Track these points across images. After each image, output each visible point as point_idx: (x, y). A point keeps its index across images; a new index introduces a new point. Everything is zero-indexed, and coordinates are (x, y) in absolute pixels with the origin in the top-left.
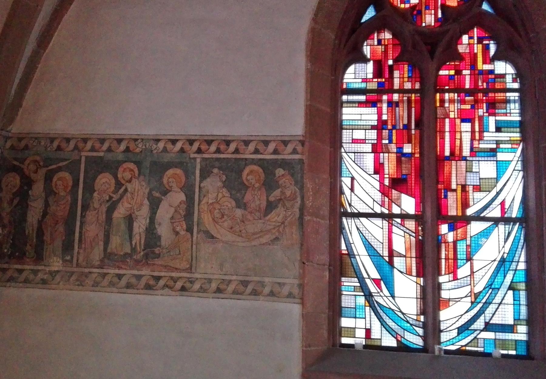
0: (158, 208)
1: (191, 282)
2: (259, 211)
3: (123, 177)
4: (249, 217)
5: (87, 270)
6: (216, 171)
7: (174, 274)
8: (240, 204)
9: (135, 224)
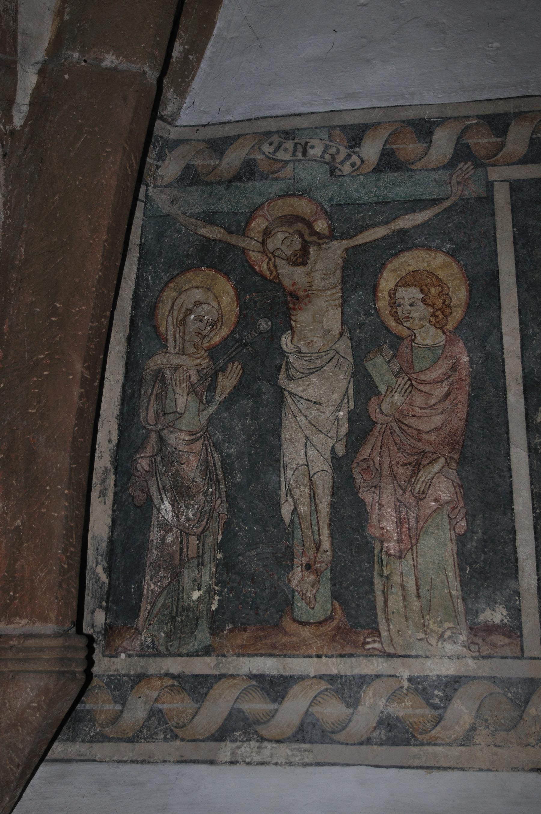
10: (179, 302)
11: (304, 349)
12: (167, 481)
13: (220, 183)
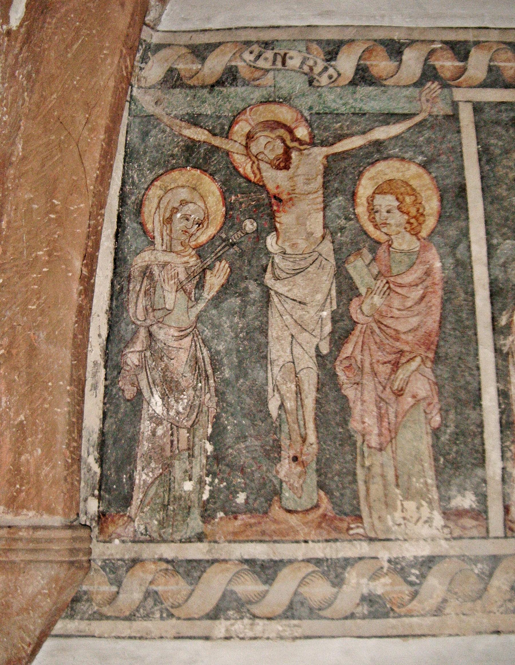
10: (165, 201)
11: (289, 251)
12: (157, 375)
13: (203, 87)
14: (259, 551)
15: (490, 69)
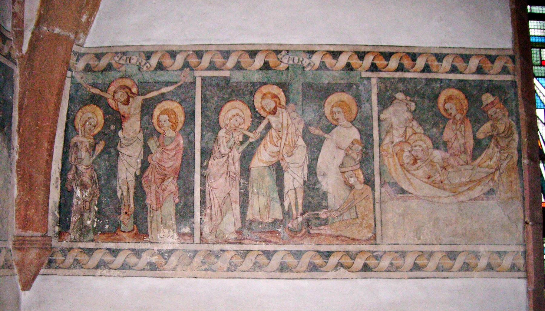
0: (319, 150)
1: (376, 258)
2: (465, 152)
3: (263, 107)
4: (452, 161)
5: (217, 247)
6: (400, 96)
7: (352, 248)
8: (438, 144)
9: (286, 175)
12: (79, 182)
13: (99, 71)
14: (112, 245)
15: (211, 62)
